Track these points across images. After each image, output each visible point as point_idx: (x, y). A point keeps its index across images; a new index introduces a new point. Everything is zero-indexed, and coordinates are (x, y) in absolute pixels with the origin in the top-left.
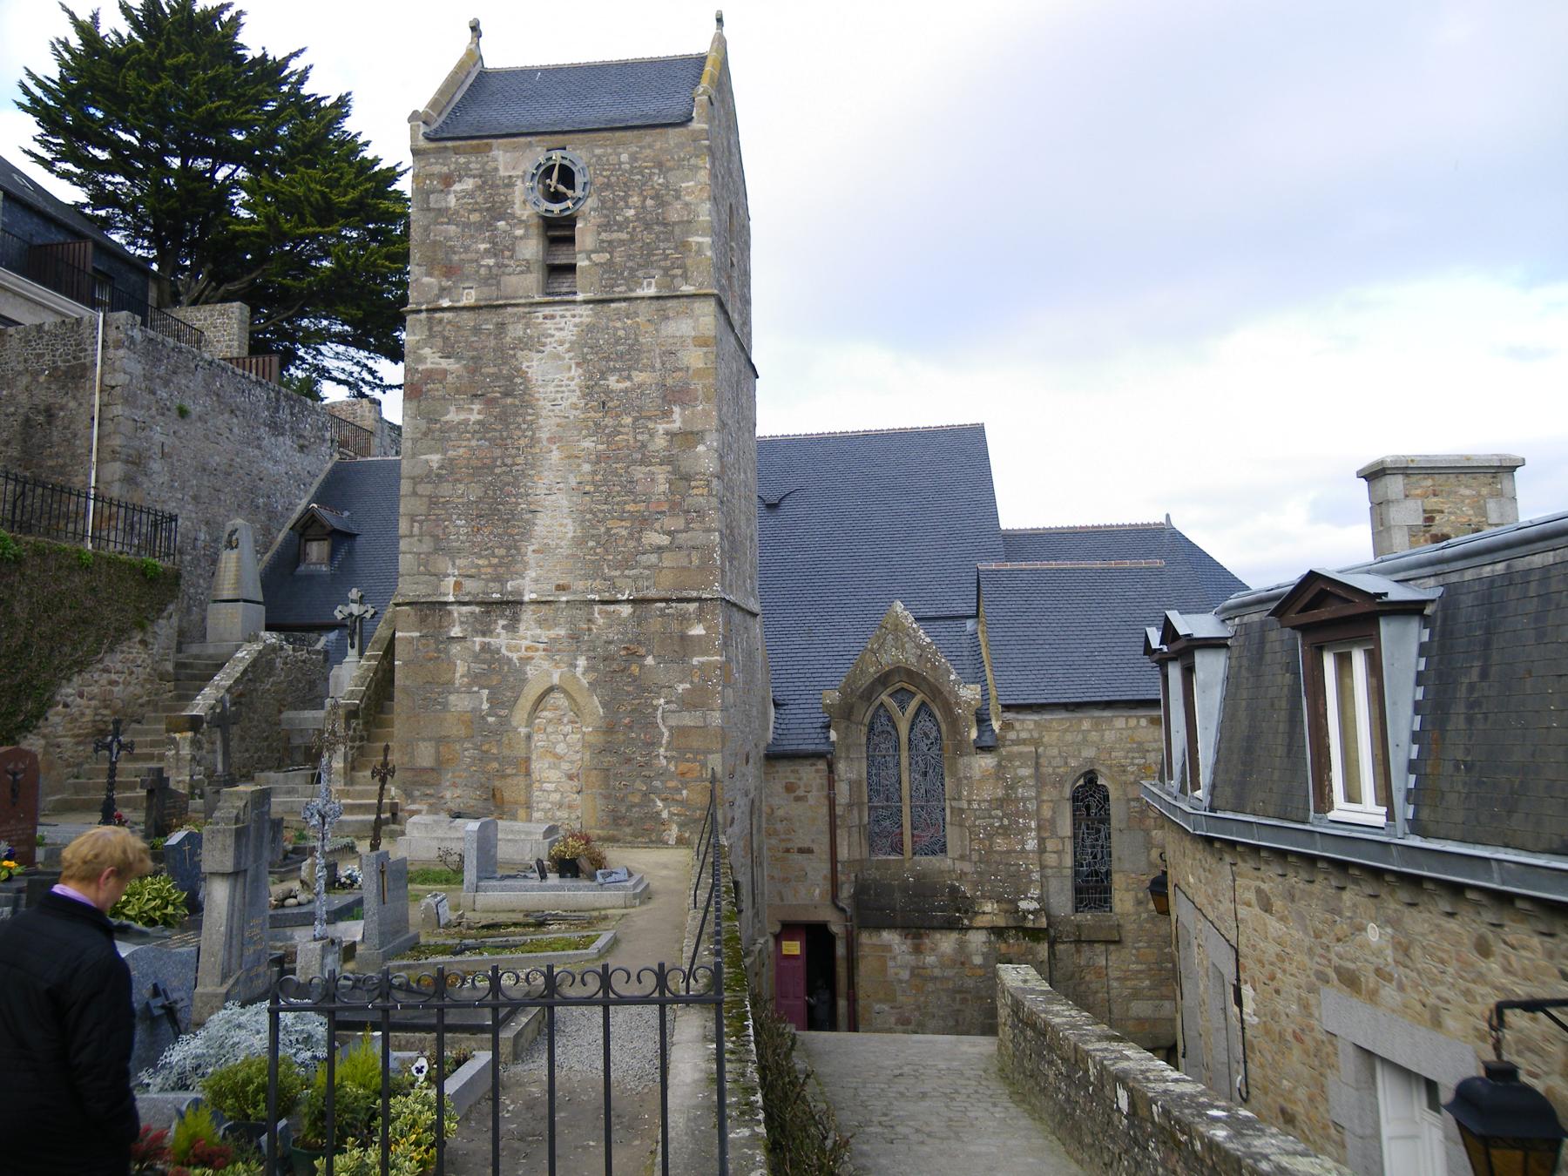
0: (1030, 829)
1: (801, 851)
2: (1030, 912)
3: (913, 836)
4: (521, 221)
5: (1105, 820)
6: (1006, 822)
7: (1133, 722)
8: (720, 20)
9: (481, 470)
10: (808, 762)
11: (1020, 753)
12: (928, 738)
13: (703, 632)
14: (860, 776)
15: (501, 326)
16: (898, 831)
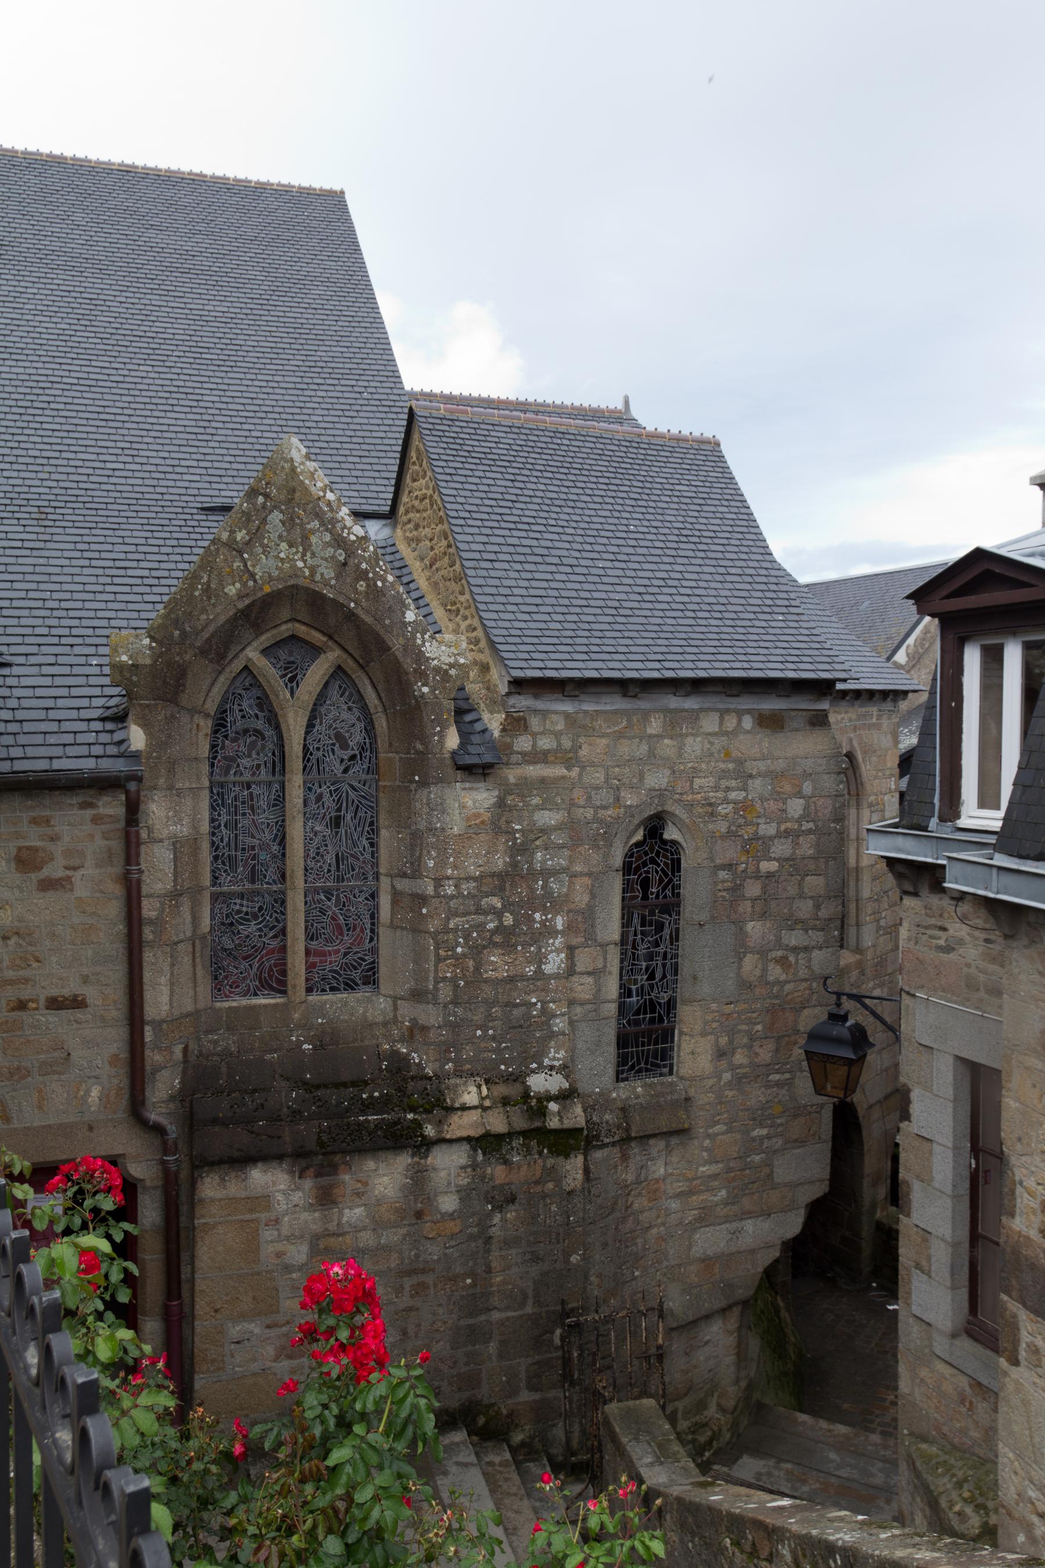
0: (553, 933)
1: (55, 1004)
2: (550, 1098)
3: (308, 952)
5: (672, 906)
6: (508, 919)
7: (731, 723)
10: (75, 800)
11: (543, 780)
12: (345, 746)
14: (195, 829)
16: (275, 944)
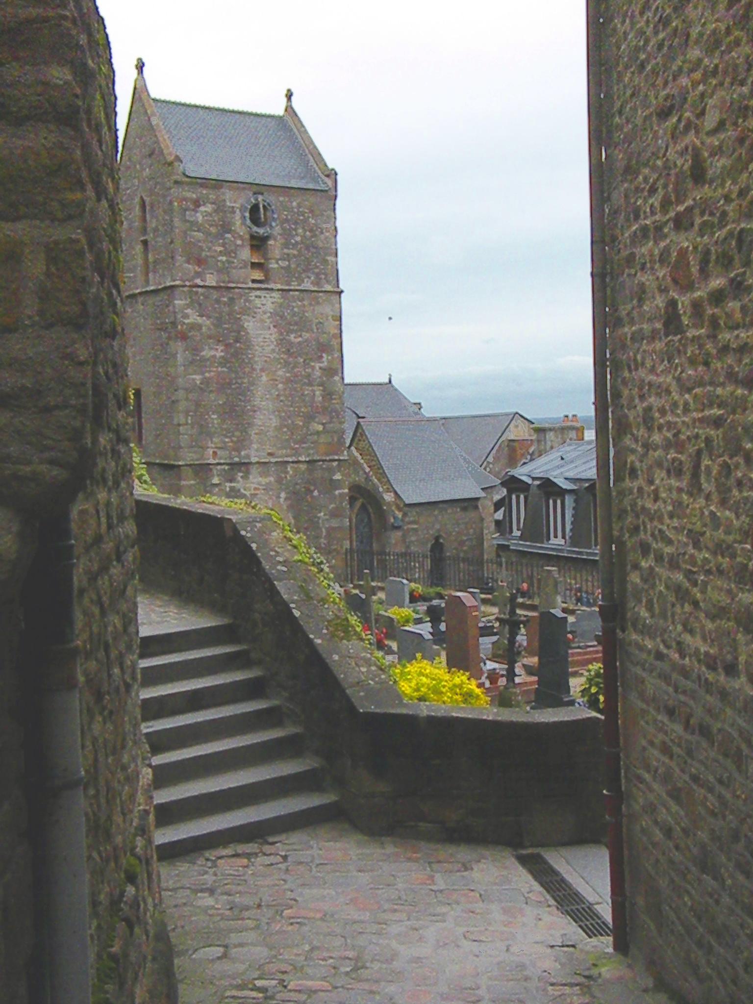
4: (240, 236)
8: (289, 95)
9: (223, 386)
13: (340, 478)
15: (232, 300)
